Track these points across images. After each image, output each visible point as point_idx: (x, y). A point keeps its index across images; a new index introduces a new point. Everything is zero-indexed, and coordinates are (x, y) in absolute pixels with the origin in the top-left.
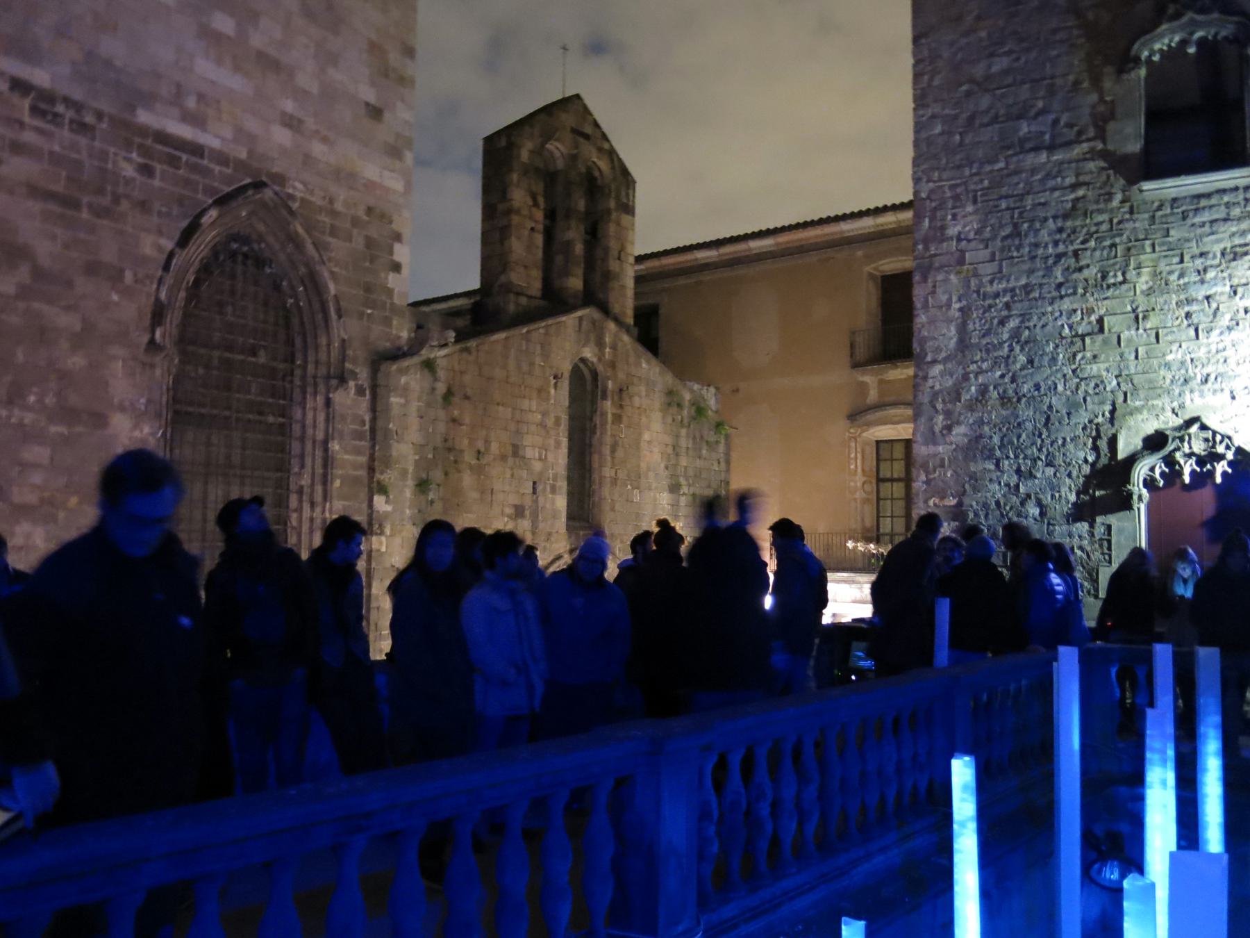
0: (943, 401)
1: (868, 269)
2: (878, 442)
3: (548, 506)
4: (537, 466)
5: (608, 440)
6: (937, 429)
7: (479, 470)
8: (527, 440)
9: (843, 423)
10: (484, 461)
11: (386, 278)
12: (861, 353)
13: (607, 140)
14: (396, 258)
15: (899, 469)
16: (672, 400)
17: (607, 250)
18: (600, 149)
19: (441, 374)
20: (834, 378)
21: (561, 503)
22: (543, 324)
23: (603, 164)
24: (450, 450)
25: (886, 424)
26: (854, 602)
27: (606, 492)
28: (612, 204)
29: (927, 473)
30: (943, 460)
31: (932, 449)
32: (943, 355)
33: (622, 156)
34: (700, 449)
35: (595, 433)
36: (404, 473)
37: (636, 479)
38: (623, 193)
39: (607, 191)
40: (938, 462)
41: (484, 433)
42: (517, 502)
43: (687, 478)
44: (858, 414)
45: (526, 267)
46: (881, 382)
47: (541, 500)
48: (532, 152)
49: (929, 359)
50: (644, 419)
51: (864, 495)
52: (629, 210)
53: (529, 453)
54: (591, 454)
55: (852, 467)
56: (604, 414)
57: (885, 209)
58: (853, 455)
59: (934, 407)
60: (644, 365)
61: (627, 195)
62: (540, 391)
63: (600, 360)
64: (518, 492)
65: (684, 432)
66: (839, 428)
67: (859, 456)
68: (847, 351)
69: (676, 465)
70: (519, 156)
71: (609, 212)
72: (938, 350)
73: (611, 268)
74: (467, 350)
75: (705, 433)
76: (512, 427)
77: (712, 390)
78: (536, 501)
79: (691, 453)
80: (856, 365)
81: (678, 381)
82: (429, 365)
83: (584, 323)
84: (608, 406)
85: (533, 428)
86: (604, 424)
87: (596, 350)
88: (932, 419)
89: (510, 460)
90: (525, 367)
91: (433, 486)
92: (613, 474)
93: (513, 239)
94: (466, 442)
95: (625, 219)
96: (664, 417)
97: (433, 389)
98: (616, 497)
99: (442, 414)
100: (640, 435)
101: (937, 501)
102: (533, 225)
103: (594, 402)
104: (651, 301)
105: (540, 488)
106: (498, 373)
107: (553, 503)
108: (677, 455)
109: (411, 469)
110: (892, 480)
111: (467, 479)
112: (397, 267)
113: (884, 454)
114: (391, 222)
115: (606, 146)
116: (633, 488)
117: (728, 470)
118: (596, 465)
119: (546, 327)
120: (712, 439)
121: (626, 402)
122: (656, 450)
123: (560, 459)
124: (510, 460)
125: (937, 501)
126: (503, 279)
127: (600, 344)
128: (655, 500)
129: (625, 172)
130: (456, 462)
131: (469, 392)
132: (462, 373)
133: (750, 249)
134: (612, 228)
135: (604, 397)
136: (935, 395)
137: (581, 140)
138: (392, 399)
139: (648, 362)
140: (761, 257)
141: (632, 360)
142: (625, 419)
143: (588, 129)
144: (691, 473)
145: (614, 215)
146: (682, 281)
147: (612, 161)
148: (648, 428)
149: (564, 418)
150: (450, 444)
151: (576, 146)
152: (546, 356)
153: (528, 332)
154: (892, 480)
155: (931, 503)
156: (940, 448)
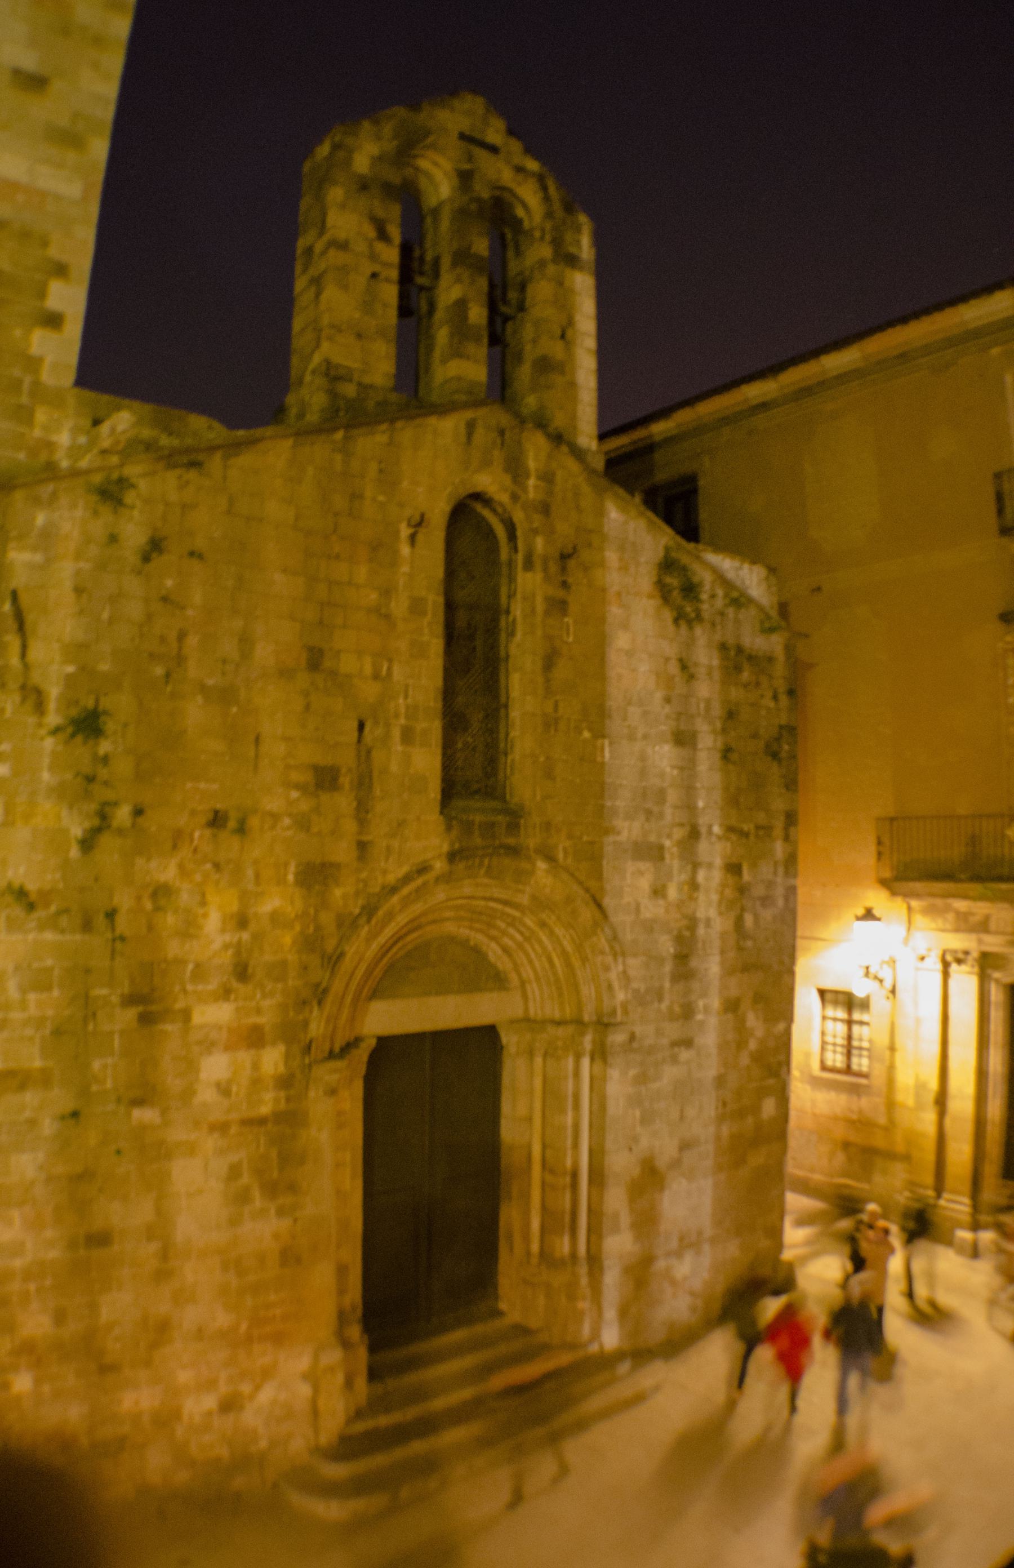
4: (370, 691)
45: (359, 336)
48: (378, 160)
53: (348, 664)
63: (515, 498)
70: (348, 162)
87: (507, 480)
92: (549, 708)
102: (377, 268)
122: (644, 668)
127: (515, 468)
128: (643, 758)
132: (185, 507)
142: (573, 608)
148: (625, 626)
151: (470, 158)
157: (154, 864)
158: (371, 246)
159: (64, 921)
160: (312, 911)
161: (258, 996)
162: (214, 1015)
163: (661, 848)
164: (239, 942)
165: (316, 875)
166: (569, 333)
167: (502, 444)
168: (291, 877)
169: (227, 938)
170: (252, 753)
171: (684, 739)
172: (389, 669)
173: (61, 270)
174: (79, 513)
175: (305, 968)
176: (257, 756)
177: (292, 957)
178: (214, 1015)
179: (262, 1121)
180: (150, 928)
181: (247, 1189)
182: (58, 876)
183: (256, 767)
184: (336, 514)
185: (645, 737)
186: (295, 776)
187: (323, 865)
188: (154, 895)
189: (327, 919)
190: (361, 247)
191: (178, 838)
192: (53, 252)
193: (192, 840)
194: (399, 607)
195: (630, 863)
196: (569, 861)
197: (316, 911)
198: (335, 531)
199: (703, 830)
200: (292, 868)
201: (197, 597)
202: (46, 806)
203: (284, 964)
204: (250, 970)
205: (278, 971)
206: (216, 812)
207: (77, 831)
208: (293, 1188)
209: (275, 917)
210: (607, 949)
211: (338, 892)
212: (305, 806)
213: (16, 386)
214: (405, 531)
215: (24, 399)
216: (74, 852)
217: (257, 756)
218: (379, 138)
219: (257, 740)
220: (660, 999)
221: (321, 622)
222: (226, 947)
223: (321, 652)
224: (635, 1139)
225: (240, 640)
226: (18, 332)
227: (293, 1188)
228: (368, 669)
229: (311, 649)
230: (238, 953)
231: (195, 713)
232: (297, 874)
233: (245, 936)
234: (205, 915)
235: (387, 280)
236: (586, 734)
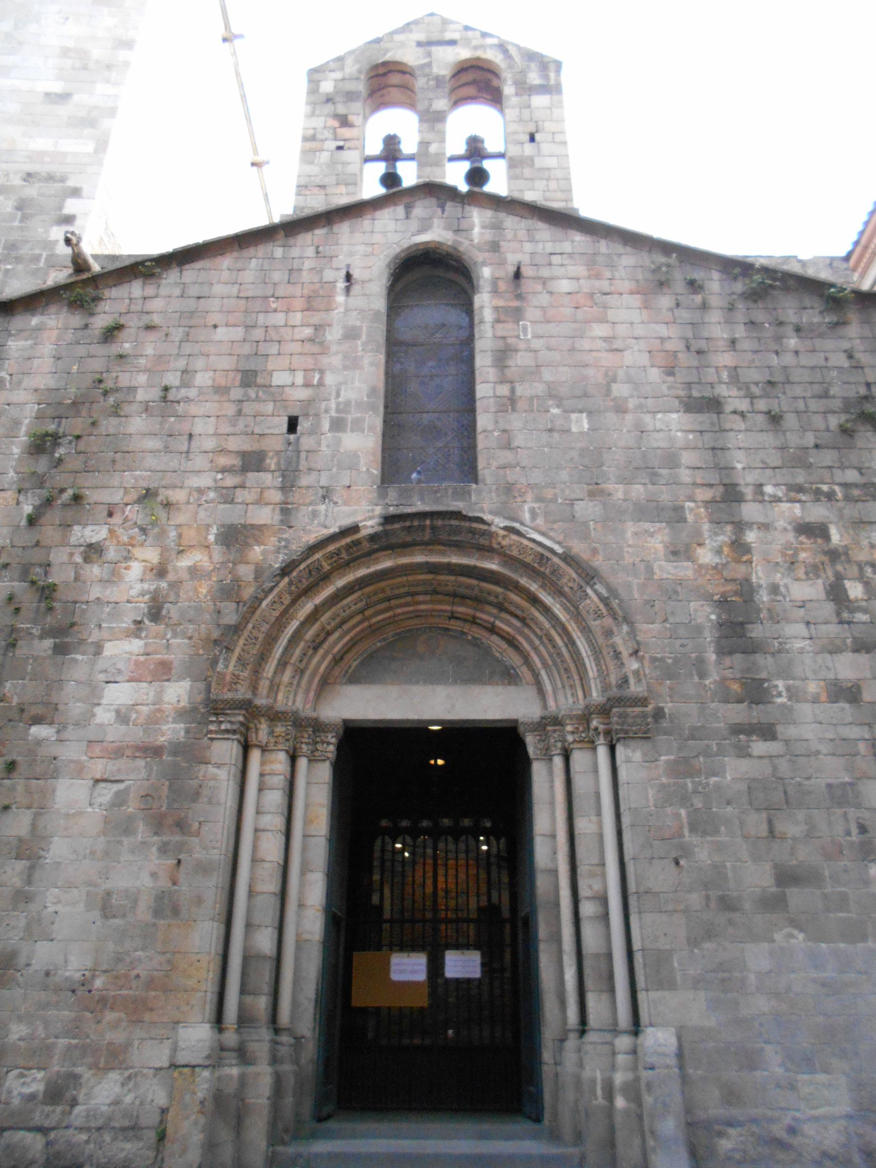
42: (246, 447)
47: (307, 442)
89: (237, 393)
102: (341, 143)
138: (10, 343)
142: (532, 313)
161: (168, 636)
162: (122, 650)
163: (679, 510)
164: (157, 591)
178: (122, 650)
179: (156, 751)
181: (131, 818)
185: (640, 408)
187: (244, 526)
189: (245, 571)
190: (328, 134)
192: (71, 183)
193: (124, 512)
195: (630, 524)
196: (540, 521)
200: (214, 530)
208: (181, 825)
210: (604, 610)
220: (702, 675)
224: (686, 851)
226: (40, 230)
227: (181, 825)
230: (154, 599)
232: (217, 535)
233: (164, 585)
236: (555, 411)
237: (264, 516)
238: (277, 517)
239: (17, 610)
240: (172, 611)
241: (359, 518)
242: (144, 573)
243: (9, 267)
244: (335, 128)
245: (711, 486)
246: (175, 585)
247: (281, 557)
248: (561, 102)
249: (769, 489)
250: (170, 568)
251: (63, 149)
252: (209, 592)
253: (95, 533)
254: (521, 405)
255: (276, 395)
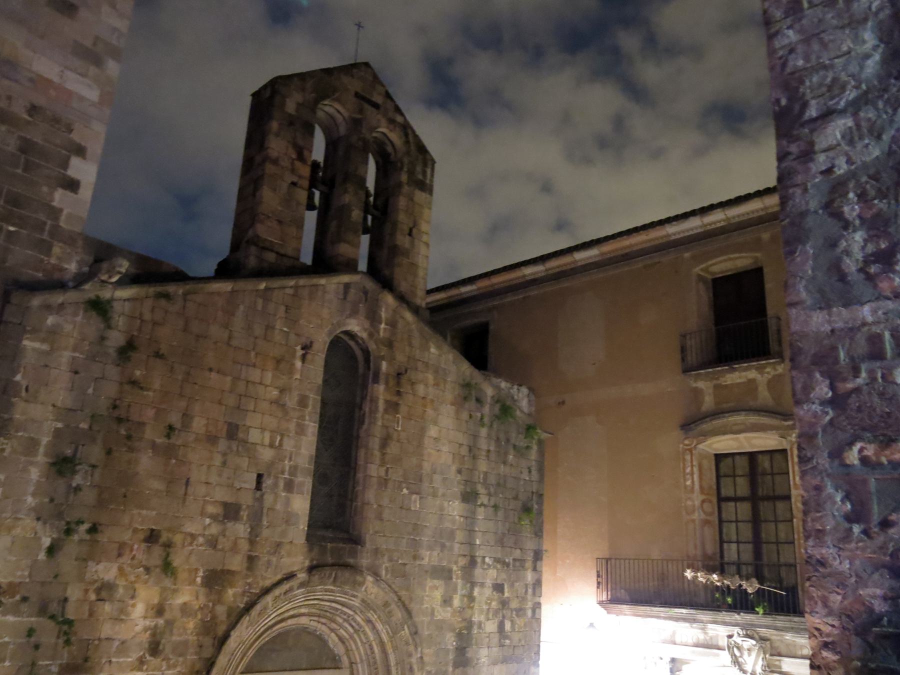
0: (862, 196)
1: (697, 270)
2: (716, 455)
3: (278, 507)
4: (267, 454)
5: (378, 431)
6: (851, 266)
7: (168, 452)
8: (253, 420)
9: (678, 434)
10: (177, 440)
11: (51, 194)
12: (692, 358)
13: (402, 114)
14: (71, 172)
15: (742, 487)
16: (468, 394)
17: (395, 225)
18: (392, 121)
19: (120, 322)
20: (664, 385)
21: (301, 505)
22: (292, 283)
23: (395, 137)
24: (119, 420)
25: (724, 433)
26: (697, 645)
27: (370, 495)
28: (404, 178)
29: (833, 379)
30: (875, 340)
31: (841, 317)
32: (851, 94)
33: (419, 132)
34: (506, 454)
35: (363, 423)
36: (32, 445)
37: (416, 481)
38: (419, 169)
39: (399, 165)
40: (861, 346)
41: (183, 404)
42: (228, 499)
43: (485, 484)
44: (693, 423)
45: (280, 222)
46: (717, 387)
47: (268, 499)
48: (299, 105)
49: (812, 112)
50: (430, 412)
51: (703, 516)
52: (426, 187)
53: (254, 436)
54: (357, 448)
55: (689, 483)
56: (374, 401)
57: (712, 208)
58: (688, 470)
59: (838, 215)
60: (433, 350)
61: (424, 173)
62: (278, 361)
63: (371, 335)
64: (231, 486)
65: (484, 432)
66: (671, 441)
67: (696, 470)
68: (678, 356)
69: (472, 470)
70: (283, 105)
71: (400, 185)
72: (836, 87)
73: (399, 243)
74: (167, 296)
75: (513, 435)
76: (231, 401)
77: (524, 390)
78: (260, 500)
79: (493, 456)
80: (686, 370)
81: (476, 373)
82: (99, 308)
83: (352, 291)
84: (380, 391)
85: (265, 405)
86: (373, 411)
87: (367, 324)
88: (834, 245)
89: (223, 444)
90: (258, 330)
91: (82, 468)
92: (383, 474)
93: (265, 187)
94: (151, 413)
95: (420, 196)
96: (457, 412)
97: (103, 338)
98: (385, 502)
99: (113, 372)
100: (423, 430)
101: (870, 451)
102: (295, 179)
103: (365, 387)
104: (482, 319)
105: (268, 482)
106: (215, 331)
107: (288, 503)
108: (474, 458)
109: (45, 440)
110: (736, 499)
111: (146, 462)
112: (73, 185)
113: (724, 469)
114: (71, 131)
115: (399, 119)
116: (412, 493)
117: (541, 480)
118: (361, 462)
119: (296, 287)
120: (522, 443)
121: (405, 388)
122: (445, 449)
123: (304, 447)
124: (223, 444)
125: (870, 451)
126: (251, 233)
127: (373, 317)
128: (442, 509)
129: (422, 149)
130: (129, 437)
131: (164, 350)
132: (155, 324)
133: (576, 261)
134: (402, 202)
135: (376, 380)
136: (838, 188)
137: (367, 106)
138: (26, 342)
139: (439, 347)
140: (587, 268)
141: (416, 342)
142: (403, 409)
143: (378, 99)
144: (492, 480)
145: (406, 189)
146: (510, 298)
147: (406, 135)
148: (435, 423)
149: (314, 399)
150: (122, 413)
151: (361, 111)
152: (292, 321)
153: (267, 289)
154: (736, 499)
155: (853, 456)
156: (866, 312)
157: (101, 567)
158: (292, 164)
159: (24, 607)
160: (211, 604)
161: (164, 668)
163: (450, 571)
164: (156, 626)
165: (216, 580)
166: (415, 231)
167: (366, 300)
168: (199, 580)
169: (148, 623)
170: (182, 492)
171: (469, 497)
172: (281, 440)
173: (80, 151)
174: (79, 319)
175: (201, 647)
176: (186, 494)
177: (192, 638)
180: (91, 614)
182: (26, 573)
183: (184, 500)
184: (256, 338)
185: (444, 495)
186: (211, 509)
187: (222, 571)
188: (98, 591)
189: (221, 610)
190: (285, 163)
191: (121, 549)
192: (75, 136)
193: (132, 550)
194: (291, 401)
195: (429, 580)
197: (214, 605)
198: (254, 349)
199: (479, 560)
200: (201, 574)
201: (157, 385)
202: (29, 522)
203: (185, 643)
204: (161, 647)
205: (180, 649)
206: (152, 530)
207: (47, 542)
209: (185, 609)
210: (411, 641)
211: (230, 592)
212: (214, 529)
213: (40, 227)
214: (300, 352)
215: (45, 236)
216: (42, 556)
217: (186, 494)
218: (303, 90)
219: (187, 483)
221: (238, 408)
222: (146, 630)
223: (237, 426)
225: (184, 415)
226: (45, 189)
228: (267, 441)
229: (230, 424)
230: (153, 635)
231: (146, 462)
232: (203, 577)
233: (161, 621)
234: (134, 606)
235: (301, 187)
236: (405, 491)
237: (236, 563)
238: (245, 565)
239: (37, 647)
240: (167, 644)
241: (295, 569)
242: (147, 611)
243: (12, 229)
244: (293, 160)
245: (465, 556)
246: (170, 623)
247: (246, 599)
248: (430, 203)
249: (487, 560)
250: (167, 607)
251: (70, 86)
252: (195, 628)
253: (106, 571)
254: (390, 485)
255: (248, 448)
